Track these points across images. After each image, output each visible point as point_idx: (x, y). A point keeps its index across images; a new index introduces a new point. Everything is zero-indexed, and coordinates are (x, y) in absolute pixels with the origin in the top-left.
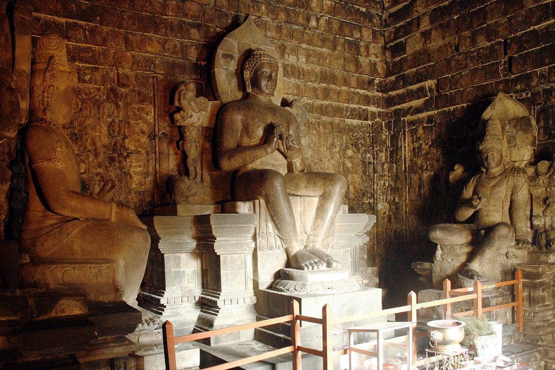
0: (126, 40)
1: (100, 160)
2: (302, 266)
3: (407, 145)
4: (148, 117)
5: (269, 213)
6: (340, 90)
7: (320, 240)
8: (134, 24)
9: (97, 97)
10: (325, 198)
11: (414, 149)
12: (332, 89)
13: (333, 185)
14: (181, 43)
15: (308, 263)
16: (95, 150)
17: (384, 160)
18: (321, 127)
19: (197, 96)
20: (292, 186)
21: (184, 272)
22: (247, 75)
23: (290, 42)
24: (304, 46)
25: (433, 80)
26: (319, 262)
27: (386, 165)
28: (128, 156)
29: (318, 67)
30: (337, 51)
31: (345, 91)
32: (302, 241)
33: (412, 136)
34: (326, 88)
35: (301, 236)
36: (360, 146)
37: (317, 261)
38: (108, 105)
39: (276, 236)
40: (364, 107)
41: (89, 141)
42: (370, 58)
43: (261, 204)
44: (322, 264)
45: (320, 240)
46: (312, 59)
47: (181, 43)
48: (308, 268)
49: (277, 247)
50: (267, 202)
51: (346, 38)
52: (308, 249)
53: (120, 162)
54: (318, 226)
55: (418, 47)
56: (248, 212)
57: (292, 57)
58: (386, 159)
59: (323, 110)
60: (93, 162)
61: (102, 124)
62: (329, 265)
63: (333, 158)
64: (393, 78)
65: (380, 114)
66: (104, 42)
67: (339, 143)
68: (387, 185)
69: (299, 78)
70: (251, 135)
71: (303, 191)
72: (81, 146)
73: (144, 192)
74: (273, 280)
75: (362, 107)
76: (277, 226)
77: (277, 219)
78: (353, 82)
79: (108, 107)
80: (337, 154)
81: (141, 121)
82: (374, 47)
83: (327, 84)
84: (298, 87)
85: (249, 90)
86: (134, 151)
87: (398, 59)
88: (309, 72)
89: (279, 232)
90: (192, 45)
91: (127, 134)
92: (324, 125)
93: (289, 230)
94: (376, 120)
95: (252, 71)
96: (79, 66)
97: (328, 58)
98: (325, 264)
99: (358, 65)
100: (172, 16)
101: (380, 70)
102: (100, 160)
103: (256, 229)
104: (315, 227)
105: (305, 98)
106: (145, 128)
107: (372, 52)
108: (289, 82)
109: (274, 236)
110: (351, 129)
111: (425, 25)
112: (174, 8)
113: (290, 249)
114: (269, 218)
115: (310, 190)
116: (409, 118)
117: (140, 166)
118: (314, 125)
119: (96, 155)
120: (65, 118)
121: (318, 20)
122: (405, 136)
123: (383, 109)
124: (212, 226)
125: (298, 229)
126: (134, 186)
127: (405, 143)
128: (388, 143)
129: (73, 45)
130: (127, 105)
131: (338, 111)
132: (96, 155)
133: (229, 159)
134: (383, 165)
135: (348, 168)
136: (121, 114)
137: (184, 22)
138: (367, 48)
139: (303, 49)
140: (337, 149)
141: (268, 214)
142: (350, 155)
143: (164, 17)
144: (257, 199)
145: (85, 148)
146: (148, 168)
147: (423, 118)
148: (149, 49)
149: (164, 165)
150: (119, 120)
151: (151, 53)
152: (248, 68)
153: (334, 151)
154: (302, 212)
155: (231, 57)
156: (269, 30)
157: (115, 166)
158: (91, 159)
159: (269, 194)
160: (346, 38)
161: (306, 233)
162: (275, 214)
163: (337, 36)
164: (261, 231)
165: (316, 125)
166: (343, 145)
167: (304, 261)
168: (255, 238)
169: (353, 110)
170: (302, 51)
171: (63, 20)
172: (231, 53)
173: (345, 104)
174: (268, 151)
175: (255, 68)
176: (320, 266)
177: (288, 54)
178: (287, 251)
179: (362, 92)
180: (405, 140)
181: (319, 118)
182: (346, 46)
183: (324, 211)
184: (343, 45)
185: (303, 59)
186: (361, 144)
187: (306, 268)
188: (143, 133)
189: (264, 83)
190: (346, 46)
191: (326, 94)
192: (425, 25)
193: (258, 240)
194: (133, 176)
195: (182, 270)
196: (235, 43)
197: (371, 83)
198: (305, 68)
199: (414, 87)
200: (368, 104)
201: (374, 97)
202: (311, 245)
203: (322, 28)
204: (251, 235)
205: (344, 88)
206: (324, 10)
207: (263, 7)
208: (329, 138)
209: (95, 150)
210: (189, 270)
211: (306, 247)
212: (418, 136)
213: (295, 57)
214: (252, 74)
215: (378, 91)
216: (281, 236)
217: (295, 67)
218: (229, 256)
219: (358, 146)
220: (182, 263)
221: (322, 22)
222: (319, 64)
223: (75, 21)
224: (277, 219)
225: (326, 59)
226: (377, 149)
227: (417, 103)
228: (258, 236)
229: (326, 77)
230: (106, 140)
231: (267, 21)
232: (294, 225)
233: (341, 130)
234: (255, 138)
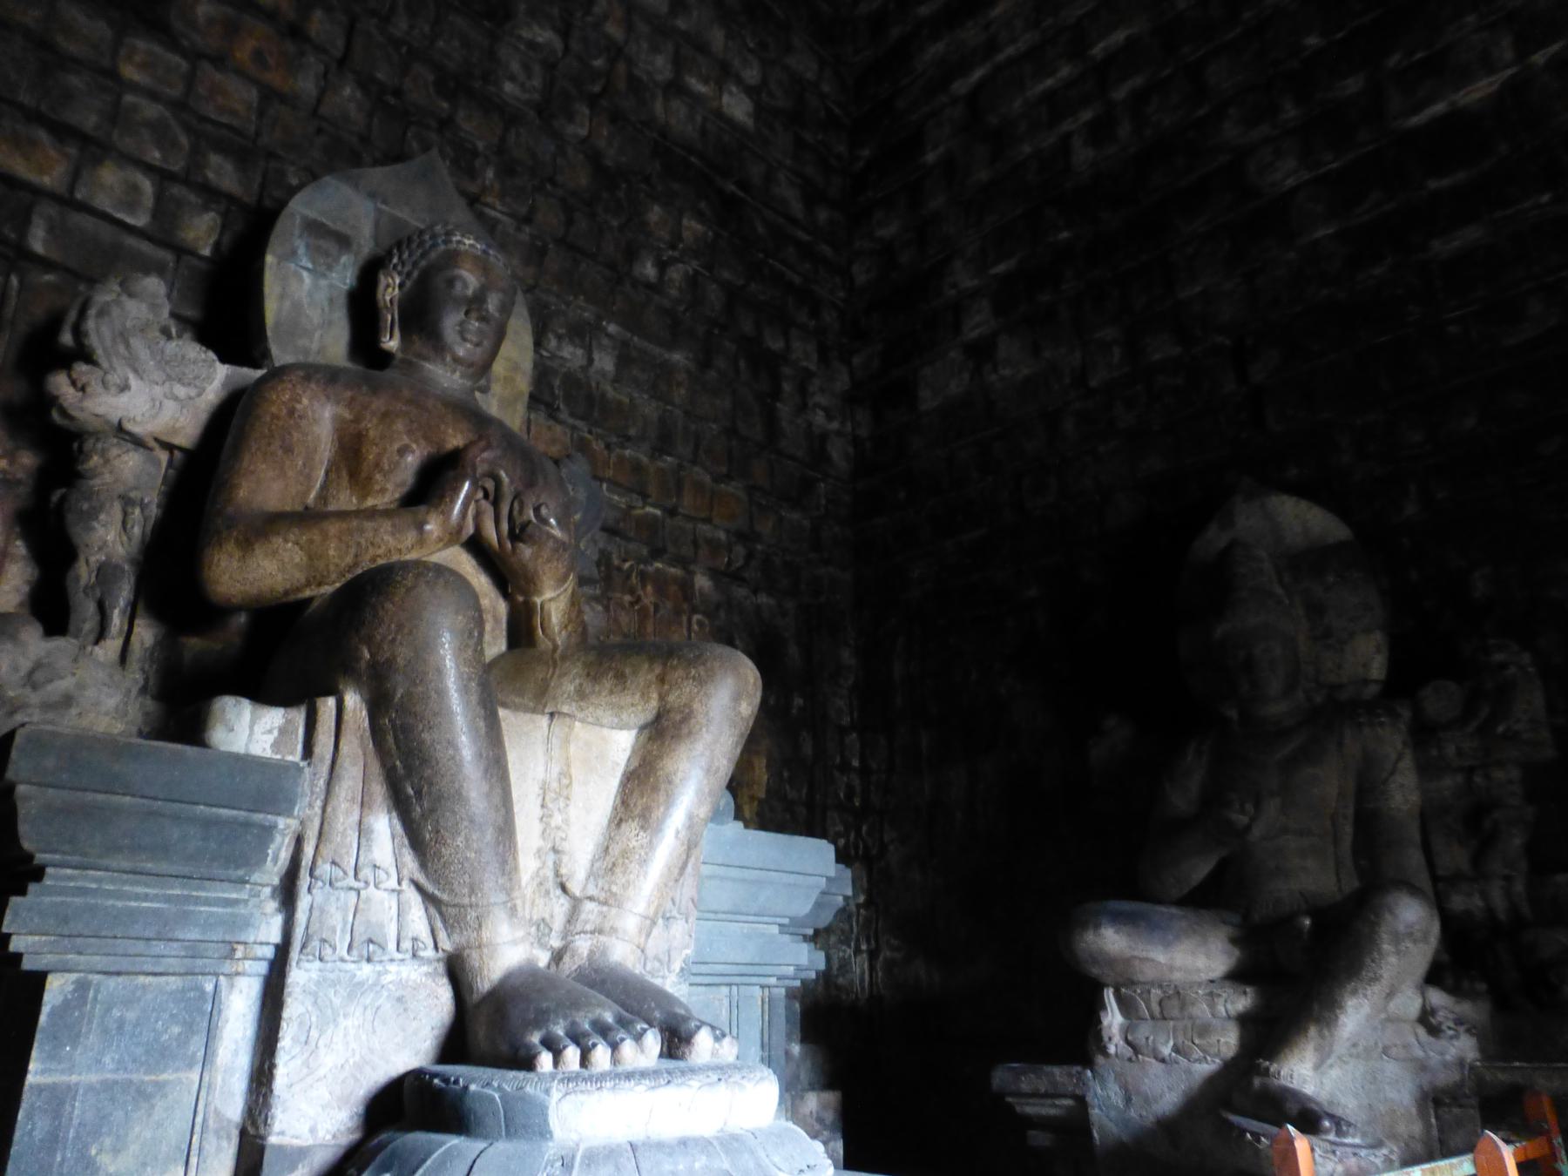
2: (529, 1047)
5: (383, 765)
7: (630, 923)
10: (662, 732)
13: (701, 682)
15: (559, 1030)
20: (521, 694)
22: (390, 289)
23: (568, 304)
24: (612, 328)
26: (623, 1023)
32: (543, 926)
35: (540, 902)
37: (609, 1017)
39: (405, 884)
43: (348, 716)
44: (638, 1038)
45: (630, 923)
48: (557, 1055)
49: (407, 945)
50: (378, 705)
52: (569, 965)
54: (625, 854)
55: (955, 387)
56: (268, 754)
57: (571, 349)
62: (676, 1041)
70: (369, 478)
74: (356, 1136)
76: (420, 836)
77: (418, 793)
85: (392, 343)
89: (423, 866)
92: (661, 584)
93: (478, 852)
95: (409, 275)
98: (653, 1041)
103: (299, 841)
104: (612, 861)
109: (393, 883)
111: (979, 321)
113: (474, 958)
114: (379, 790)
115: (598, 706)
121: (662, 266)
124: (21, 789)
125: (528, 864)
133: (246, 545)
138: (802, 390)
139: (608, 335)
141: (375, 768)
144: (328, 693)
152: (395, 267)
154: (555, 785)
159: (390, 662)
161: (564, 888)
162: (409, 768)
164: (326, 851)
167: (541, 1019)
168: (287, 894)
170: (605, 341)
174: (428, 527)
175: (423, 263)
176: (628, 1048)
177: (560, 338)
178: (456, 970)
182: (742, 364)
183: (655, 789)
185: (605, 362)
187: (545, 1060)
189: (450, 322)
190: (742, 364)
192: (979, 321)
193: (303, 903)
202: (583, 945)
203: (674, 292)
204: (272, 872)
206: (680, 239)
207: (490, 174)
211: (558, 957)
213: (580, 352)
214: (408, 284)
216: (430, 888)
221: (676, 274)
224: (418, 793)
228: (304, 880)
232: (506, 831)
234: (383, 491)
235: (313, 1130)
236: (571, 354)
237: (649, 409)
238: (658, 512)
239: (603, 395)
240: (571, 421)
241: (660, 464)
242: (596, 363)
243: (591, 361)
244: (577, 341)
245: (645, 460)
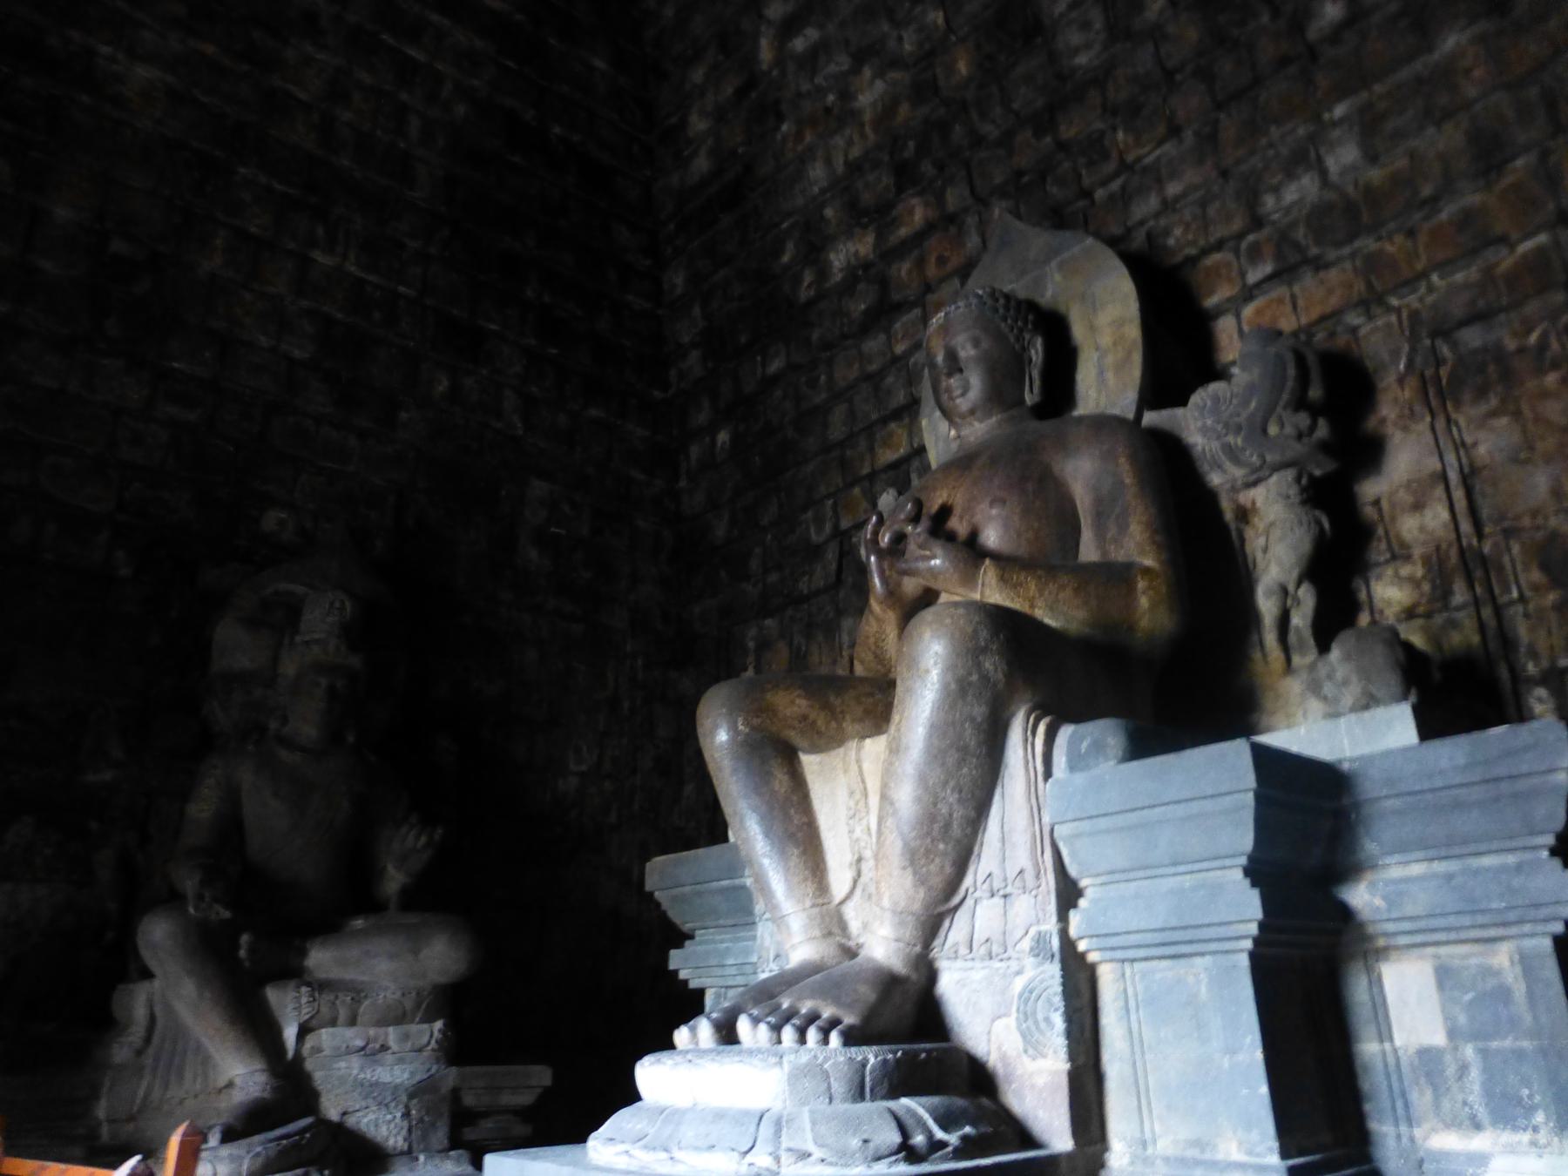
23: (1271, 145)
24: (1339, 111)
156: (1174, 175)
185: (1343, 156)
231: (1158, 158)
236: (1301, 190)
237: (1446, 139)
238: (1542, 238)
240: (1346, 250)
241: (1508, 180)
243: (1323, 173)
245: (1473, 199)
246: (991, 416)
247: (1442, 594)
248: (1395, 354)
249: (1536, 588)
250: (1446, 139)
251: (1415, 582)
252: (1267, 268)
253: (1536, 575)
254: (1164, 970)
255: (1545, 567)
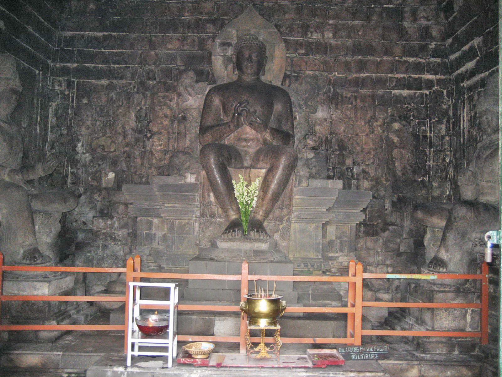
0: (150, 42)
1: (127, 140)
3: (465, 115)
4: (171, 103)
6: (381, 60)
8: (156, 28)
9: (129, 90)
11: (471, 117)
12: (369, 60)
14: (199, 38)
16: (124, 132)
17: (444, 133)
18: (358, 101)
19: (197, 82)
21: (155, 234)
25: (480, 37)
27: (447, 138)
28: (151, 137)
29: (350, 41)
30: (373, 22)
31: (388, 61)
33: (469, 104)
34: (361, 61)
36: (411, 118)
38: (137, 96)
40: (417, 76)
41: (120, 126)
42: (420, 22)
46: (341, 33)
47: (199, 38)
51: (385, 6)
53: (144, 141)
57: (316, 35)
58: (446, 131)
59: (359, 83)
60: (122, 142)
61: (131, 112)
63: (373, 132)
64: (450, 41)
65: (439, 81)
66: (132, 46)
67: (382, 116)
68: (448, 161)
69: (326, 54)
71: (261, 164)
72: (113, 130)
73: (162, 167)
75: (413, 76)
78: (398, 50)
79: (137, 98)
80: (379, 128)
81: (165, 107)
82: (424, 10)
83: (363, 55)
84: (325, 63)
86: (157, 132)
87: (451, 19)
88: (337, 47)
90: (209, 38)
91: (151, 119)
94: (434, 89)
96: (114, 67)
97: (362, 30)
99: (402, 32)
100: (188, 16)
101: (434, 33)
102: (127, 140)
105: (336, 73)
106: (168, 112)
107: (422, 16)
108: (315, 59)
110: (399, 100)
112: (190, 10)
116: (466, 84)
117: (161, 145)
118: (350, 99)
119: (125, 137)
120: (5, 110)
122: (464, 104)
123: (444, 75)
126: (154, 161)
127: (464, 112)
128: (451, 113)
129: (109, 52)
130: (153, 95)
131: (381, 82)
132: (125, 137)
134: (443, 137)
135: (393, 142)
136: (148, 102)
137: (200, 19)
140: (379, 123)
142: (397, 128)
143: (183, 18)
145: (116, 132)
146: (168, 146)
147: (478, 81)
148: (170, 46)
149: (181, 144)
150: (146, 107)
151: (171, 49)
153: (374, 124)
155: (229, 44)
157: (139, 145)
158: (120, 140)
160: (385, 6)
163: (373, 6)
165: (352, 99)
166: (388, 118)
169: (398, 80)
171: (101, 34)
172: (229, 41)
173: (389, 75)
177: (312, 33)
179: (411, 60)
180: (464, 108)
181: (357, 92)
184: (380, 15)
185: (329, 35)
186: (413, 116)
188: (166, 116)
190: (384, 15)
191: (362, 66)
194: (154, 153)
195: (153, 232)
196: (234, 32)
197: (423, 48)
198: (333, 42)
199: (466, 48)
200: (422, 71)
201: (429, 64)
205: (385, 58)
208: (368, 112)
209: (124, 132)
210: (160, 233)
212: (474, 103)
213: (319, 34)
215: (433, 57)
217: (320, 44)
218: (177, 222)
219: (408, 118)
220: (154, 226)
222: (349, 37)
223: (110, 33)
225: (358, 31)
226: (434, 120)
227: (470, 65)
229: (357, 49)
230: (133, 124)
233: (385, 102)
235: (205, 245)
239: (330, 44)
242: (326, 36)
243: (323, 36)
244: (318, 31)
246: (254, 76)
247: (320, 146)
248: (324, 87)
249: (336, 149)
250: (350, 42)
251: (315, 142)
252: (303, 52)
253: (337, 147)
254: (304, 226)
255: (338, 146)
